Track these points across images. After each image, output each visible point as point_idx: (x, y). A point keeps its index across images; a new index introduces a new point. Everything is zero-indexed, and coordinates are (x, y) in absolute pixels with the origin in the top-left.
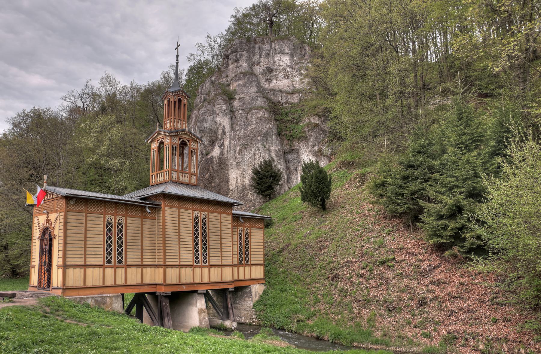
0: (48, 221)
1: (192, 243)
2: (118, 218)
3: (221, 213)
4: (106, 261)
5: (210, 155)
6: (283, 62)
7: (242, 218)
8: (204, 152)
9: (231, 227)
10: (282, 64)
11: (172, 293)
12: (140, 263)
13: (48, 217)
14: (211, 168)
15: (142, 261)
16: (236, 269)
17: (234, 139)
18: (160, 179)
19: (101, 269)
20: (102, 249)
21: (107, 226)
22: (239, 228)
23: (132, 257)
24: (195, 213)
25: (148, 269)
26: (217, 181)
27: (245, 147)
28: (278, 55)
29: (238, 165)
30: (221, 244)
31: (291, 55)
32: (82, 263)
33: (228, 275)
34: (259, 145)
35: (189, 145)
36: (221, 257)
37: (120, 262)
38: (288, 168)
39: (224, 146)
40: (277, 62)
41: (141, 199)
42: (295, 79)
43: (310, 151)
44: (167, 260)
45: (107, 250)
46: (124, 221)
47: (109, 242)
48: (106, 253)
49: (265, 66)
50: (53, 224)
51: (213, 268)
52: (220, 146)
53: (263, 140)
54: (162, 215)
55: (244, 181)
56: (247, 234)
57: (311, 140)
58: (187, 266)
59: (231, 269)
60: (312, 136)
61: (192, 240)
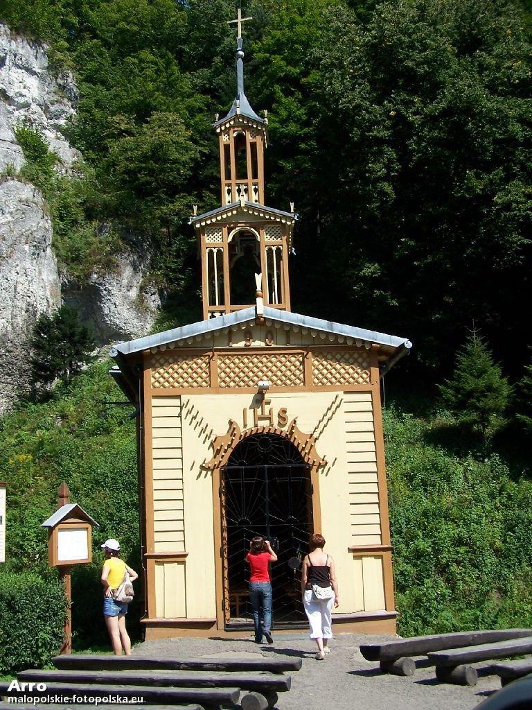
10: (24, 92)
31: (41, 78)
34: (28, 265)
53: (33, 254)
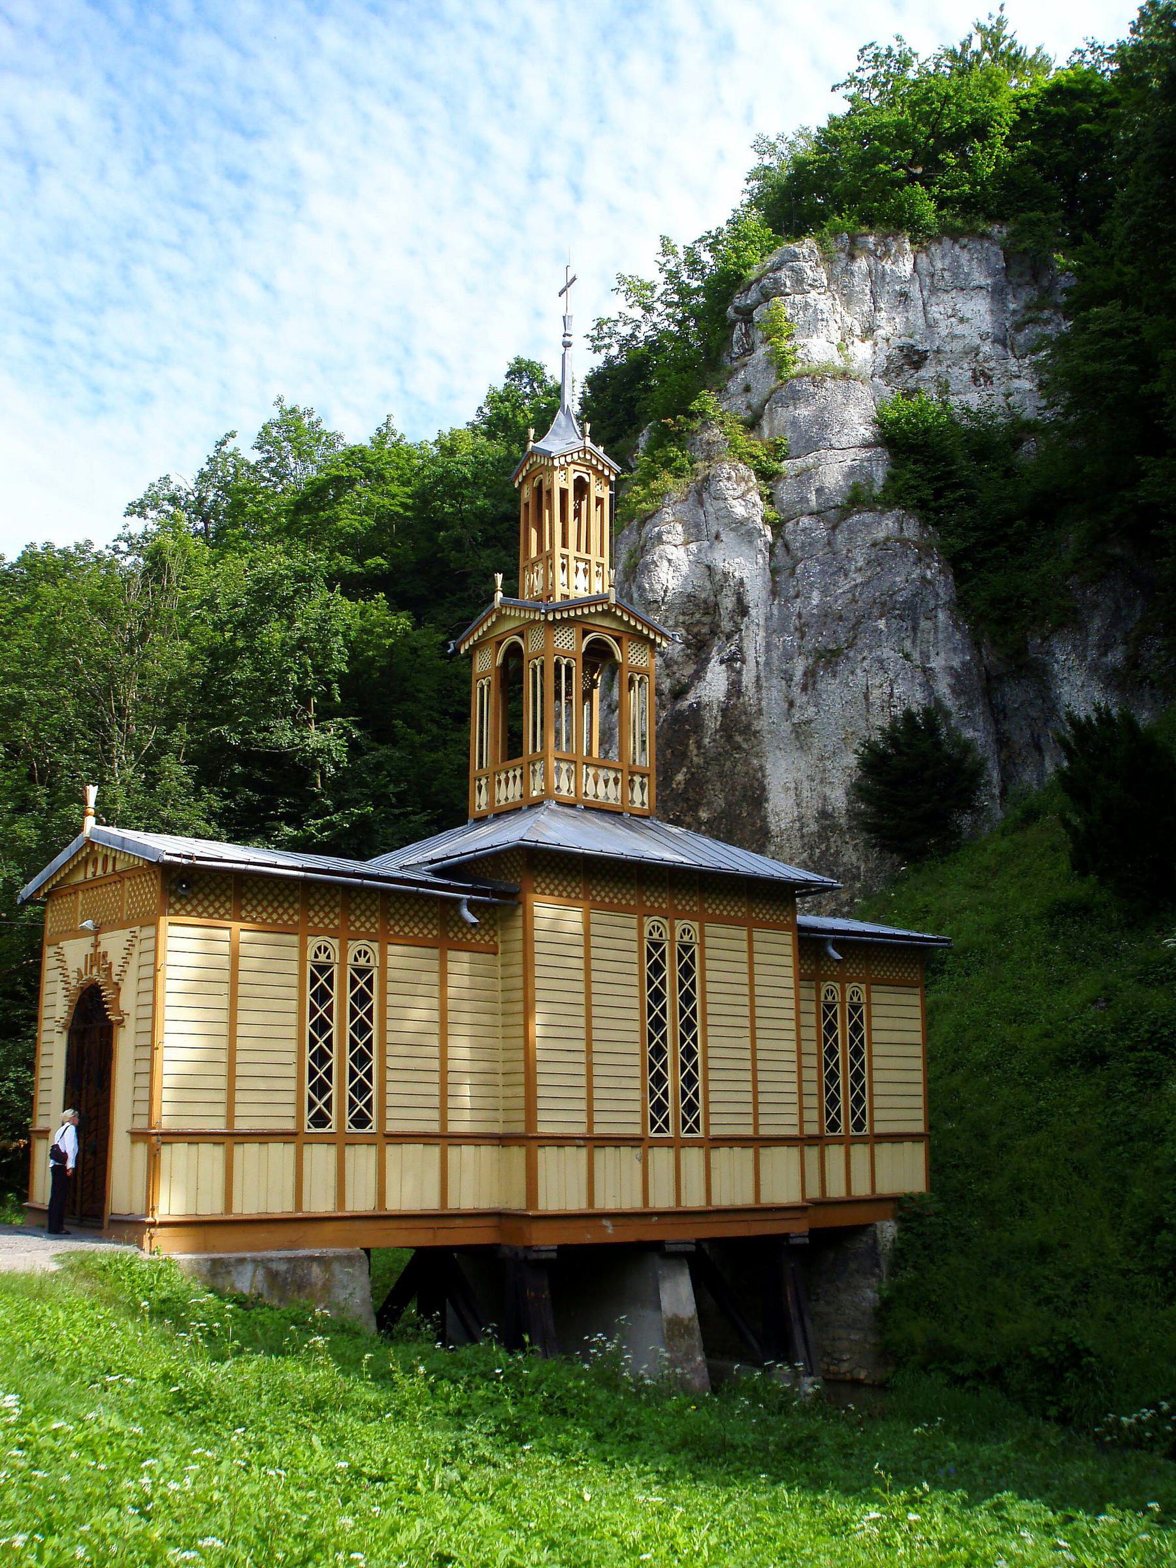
0: (97, 959)
1: (637, 1048)
2: (354, 947)
3: (751, 924)
4: (307, 1117)
5: (691, 698)
6: (962, 320)
7: (837, 945)
8: (666, 685)
9: (791, 983)
10: (960, 329)
11: (563, 1249)
12: (435, 1128)
13: (96, 945)
14: (692, 747)
15: (444, 1121)
16: (812, 1153)
17: (783, 629)
18: (509, 793)
19: (290, 1149)
20: (292, 1071)
21: (314, 980)
22: (825, 987)
23: (404, 1103)
24: (648, 922)
25: (468, 1151)
26: (720, 802)
27: (828, 659)
28: (946, 297)
29: (801, 733)
30: (754, 1050)
31: (997, 294)
32: (218, 1125)
33: (783, 1181)
34: (887, 652)
35: (619, 656)
36: (756, 1103)
37: (361, 1121)
38: (1002, 742)
39: (743, 662)
40: (942, 324)
41: (437, 873)
42: (1017, 383)
43: (1094, 669)
44: (541, 1116)
45: (313, 1073)
46: (375, 961)
47: (321, 1042)
48: (307, 1086)
49: (896, 342)
50: (116, 969)
51: (724, 1151)
52: (729, 661)
54: (519, 934)
55: (825, 798)
56: (855, 1008)
57: (1097, 623)
58: (617, 1141)
59: (794, 1152)
60: (1096, 606)
61: (636, 1037)
